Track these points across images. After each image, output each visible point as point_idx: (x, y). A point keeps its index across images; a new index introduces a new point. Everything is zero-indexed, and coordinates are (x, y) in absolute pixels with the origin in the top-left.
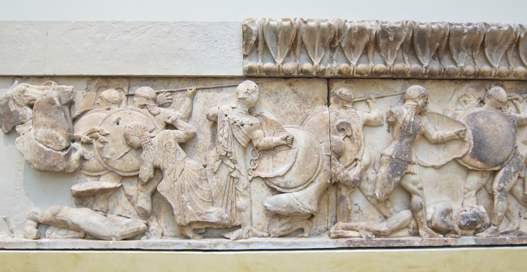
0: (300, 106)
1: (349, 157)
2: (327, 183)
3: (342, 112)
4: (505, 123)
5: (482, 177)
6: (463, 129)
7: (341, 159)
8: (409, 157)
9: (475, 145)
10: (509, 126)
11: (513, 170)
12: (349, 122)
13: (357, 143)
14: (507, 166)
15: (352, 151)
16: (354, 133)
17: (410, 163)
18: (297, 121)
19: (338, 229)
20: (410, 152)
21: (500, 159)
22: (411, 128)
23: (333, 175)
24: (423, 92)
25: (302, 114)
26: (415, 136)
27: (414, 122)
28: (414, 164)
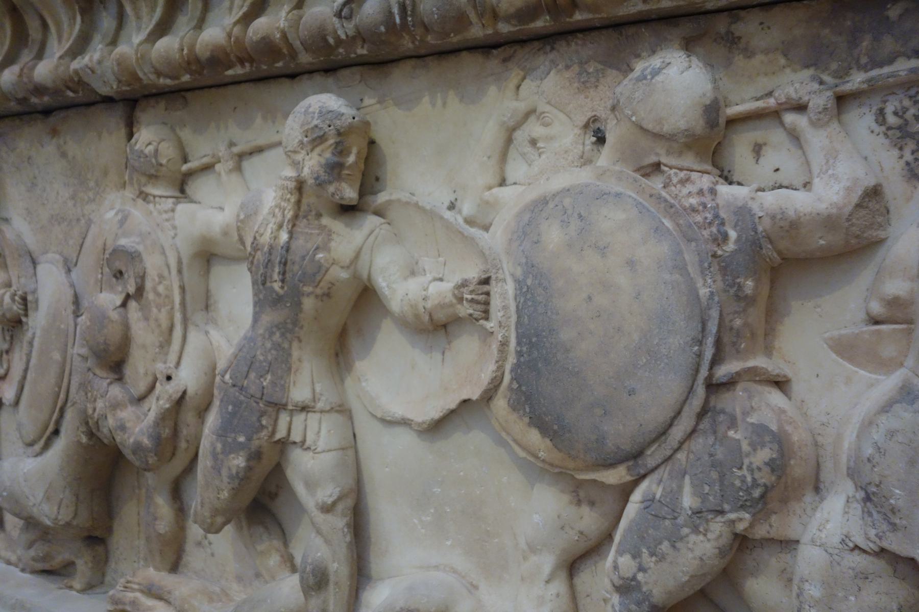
0: (73, 197)
1: (140, 366)
2: (79, 443)
3: (138, 213)
4: (653, 252)
5: (579, 503)
6: (473, 273)
7: (128, 371)
8: (273, 384)
9: (519, 354)
10: (681, 268)
11: (688, 501)
12: (140, 248)
13: (157, 320)
14: (664, 472)
15: (144, 346)
16: (149, 285)
17: (279, 407)
18: (71, 242)
19: (133, 590)
20: (282, 364)
21: (620, 432)
22: (277, 270)
23: (90, 421)
24: (315, 122)
25: (78, 220)
26: (299, 304)
27: (287, 248)
28: (304, 409)
